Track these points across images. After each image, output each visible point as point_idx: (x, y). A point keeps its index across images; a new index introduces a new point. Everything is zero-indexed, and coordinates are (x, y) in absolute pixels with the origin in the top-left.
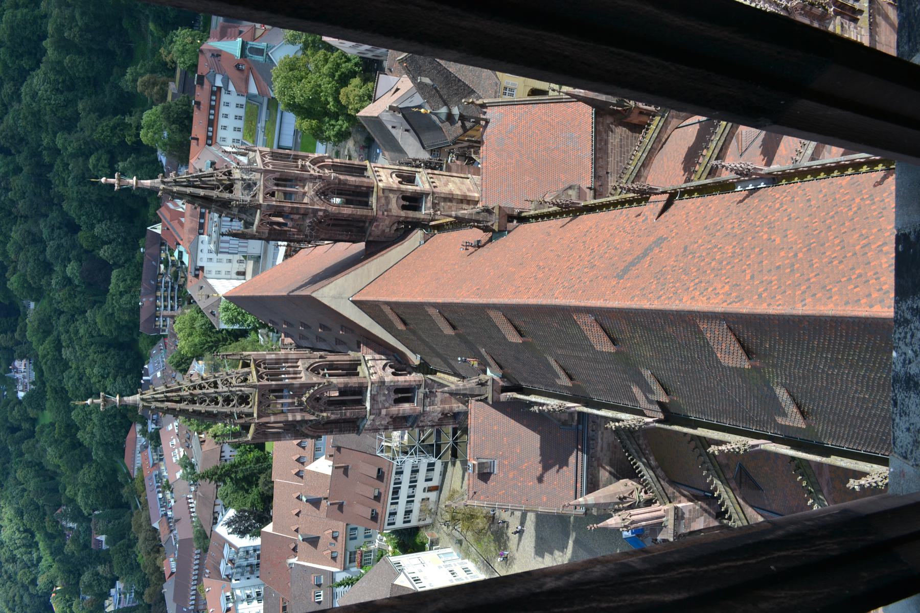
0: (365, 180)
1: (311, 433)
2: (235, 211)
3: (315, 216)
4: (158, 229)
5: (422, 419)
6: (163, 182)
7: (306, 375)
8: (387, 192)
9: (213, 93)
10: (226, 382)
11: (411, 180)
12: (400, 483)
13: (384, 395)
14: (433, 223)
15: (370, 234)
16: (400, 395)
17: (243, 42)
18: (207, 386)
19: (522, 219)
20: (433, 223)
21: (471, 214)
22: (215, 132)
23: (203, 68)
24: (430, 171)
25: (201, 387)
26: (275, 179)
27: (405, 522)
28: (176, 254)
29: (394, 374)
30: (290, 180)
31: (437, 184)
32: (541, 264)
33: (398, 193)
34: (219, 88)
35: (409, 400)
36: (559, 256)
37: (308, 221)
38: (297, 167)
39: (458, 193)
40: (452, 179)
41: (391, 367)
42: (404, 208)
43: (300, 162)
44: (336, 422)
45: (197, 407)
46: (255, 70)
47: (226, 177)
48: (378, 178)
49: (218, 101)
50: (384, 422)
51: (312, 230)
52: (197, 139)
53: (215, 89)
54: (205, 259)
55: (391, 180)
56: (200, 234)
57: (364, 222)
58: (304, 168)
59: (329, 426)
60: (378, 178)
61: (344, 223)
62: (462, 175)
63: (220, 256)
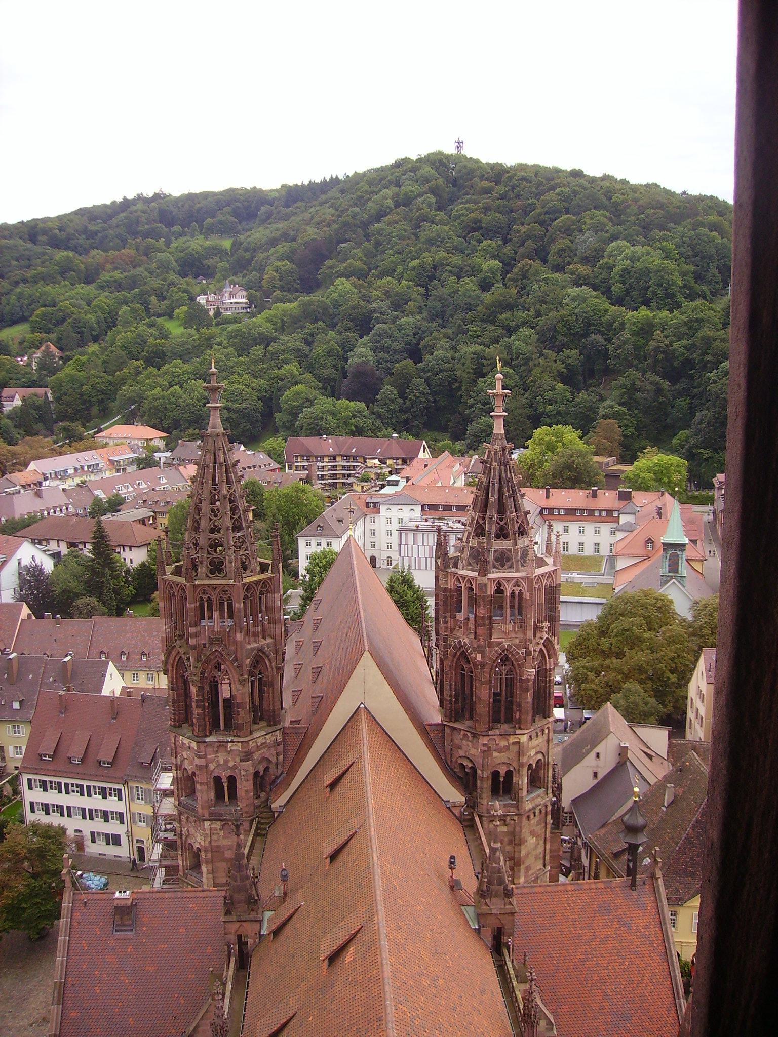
0: (530, 717)
1: (171, 660)
2: (473, 543)
3: (474, 650)
4: (424, 455)
5: (192, 819)
6: (504, 449)
7: (253, 649)
8: (515, 749)
9: (610, 512)
10: (241, 542)
11: (535, 781)
12: (89, 795)
13: (226, 761)
14: (477, 819)
15: (453, 729)
16: (226, 785)
17: (684, 545)
18: (236, 517)
19: (498, 948)
20: (477, 819)
21: (499, 871)
22: (559, 519)
23: (640, 498)
24: (549, 808)
25: (234, 510)
26: (521, 593)
27: (32, 804)
28: (393, 478)
29: (256, 774)
30: (520, 613)
31: (534, 821)
32: (441, 982)
33: (515, 764)
34: (617, 520)
35: (219, 795)
36: (455, 1009)
37: (467, 641)
38: (539, 621)
39: (523, 853)
40: (542, 842)
41: (267, 769)
42: (496, 774)
43: (546, 624)
44: (187, 694)
45: (206, 507)
46: (647, 564)
47: (516, 528)
48: (534, 735)
49: (600, 520)
50: (186, 764)
51: (455, 647)
52: (548, 497)
53: (615, 514)
54: (389, 515)
55: (533, 753)
56: (423, 509)
57: (471, 718)
58: (537, 629)
59: (181, 685)
60: (534, 735)
61: (467, 690)
62: (547, 858)
63: (395, 534)
